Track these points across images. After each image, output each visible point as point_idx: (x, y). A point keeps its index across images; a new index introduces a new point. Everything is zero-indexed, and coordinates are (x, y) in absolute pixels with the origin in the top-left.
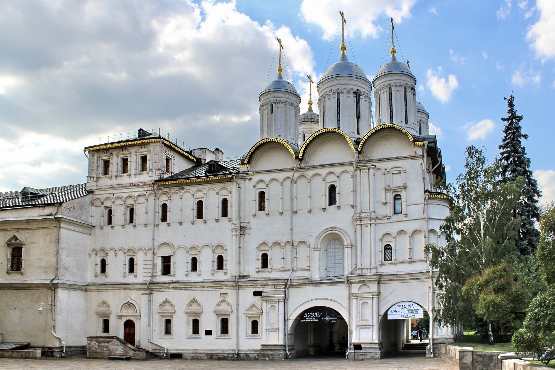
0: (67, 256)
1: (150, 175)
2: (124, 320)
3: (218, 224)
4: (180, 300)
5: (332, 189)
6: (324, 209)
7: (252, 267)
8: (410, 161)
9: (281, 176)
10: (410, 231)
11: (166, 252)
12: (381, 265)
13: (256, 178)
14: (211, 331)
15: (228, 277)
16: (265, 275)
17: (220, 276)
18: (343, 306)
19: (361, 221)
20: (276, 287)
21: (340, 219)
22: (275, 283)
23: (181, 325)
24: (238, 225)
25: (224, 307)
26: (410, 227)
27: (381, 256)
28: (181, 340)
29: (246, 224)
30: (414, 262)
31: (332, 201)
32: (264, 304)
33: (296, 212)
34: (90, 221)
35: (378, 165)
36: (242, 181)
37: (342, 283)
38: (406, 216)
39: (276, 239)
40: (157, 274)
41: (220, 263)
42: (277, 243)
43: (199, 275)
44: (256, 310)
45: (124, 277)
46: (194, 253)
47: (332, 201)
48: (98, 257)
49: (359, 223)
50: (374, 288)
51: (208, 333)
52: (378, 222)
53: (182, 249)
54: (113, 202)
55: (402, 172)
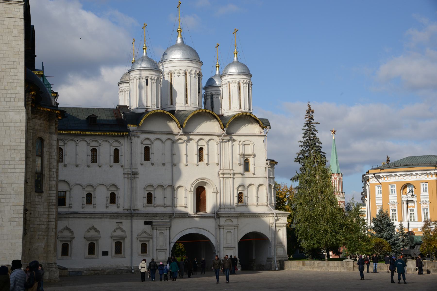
3: (112, 168)
4: (80, 228)
7: (140, 203)
8: (257, 137)
10: (257, 185)
14: (108, 252)
15: (120, 210)
16: (150, 209)
17: (113, 208)
18: (211, 234)
19: (223, 175)
20: (162, 218)
22: (162, 215)
24: (130, 170)
25: (119, 233)
28: (79, 260)
29: (136, 171)
30: (260, 205)
32: (155, 231)
36: (133, 138)
38: (254, 174)
39: (160, 182)
41: (113, 198)
42: (161, 186)
43: (95, 207)
44: (146, 235)
46: (90, 189)
47: (200, 158)
51: (105, 253)
53: (79, 187)
55: (251, 144)
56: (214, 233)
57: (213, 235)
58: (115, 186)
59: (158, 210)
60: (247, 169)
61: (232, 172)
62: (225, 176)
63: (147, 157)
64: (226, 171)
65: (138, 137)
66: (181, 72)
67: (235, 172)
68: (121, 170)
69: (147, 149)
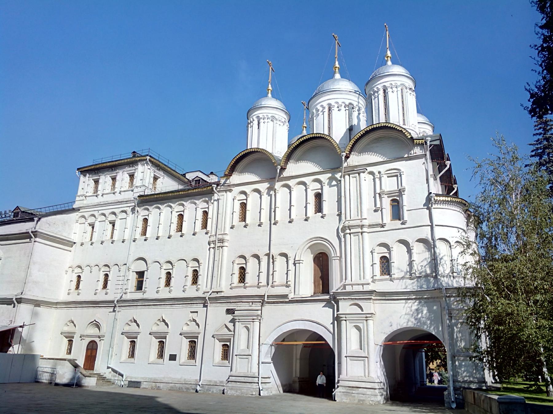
0: (39, 271)
1: (134, 191)
4: (148, 318)
11: (141, 266)
15: (200, 294)
20: (251, 303)
21: (326, 228)
23: (147, 347)
25: (193, 328)
26: (410, 236)
34: (72, 238)
35: (370, 169)
40: (128, 291)
48: (74, 274)
49: (348, 231)
51: (173, 358)
57: (330, 333)
58: (197, 260)
62: (352, 231)
64: (352, 223)
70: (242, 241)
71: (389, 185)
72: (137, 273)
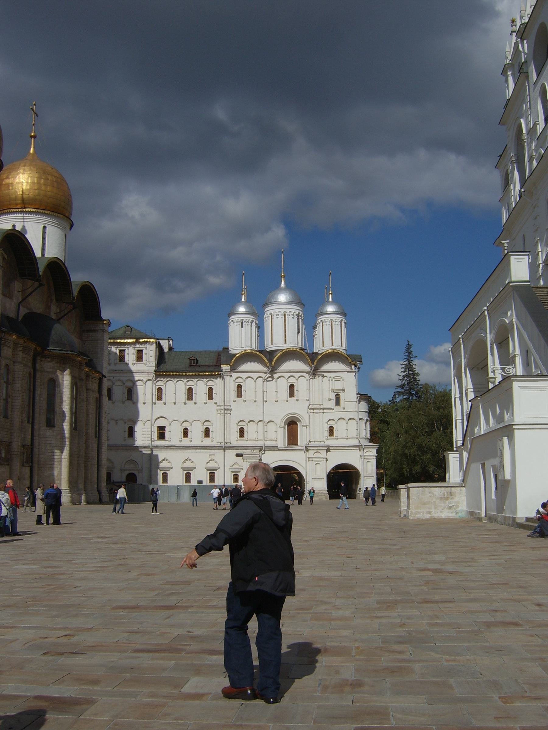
2: (127, 473)
5: (292, 386)
6: (287, 401)
9: (255, 376)
10: (347, 419)
12: (327, 439)
13: (235, 375)
15: (214, 444)
17: (207, 442)
25: (212, 465)
26: (347, 416)
27: (327, 433)
29: (228, 407)
31: (292, 394)
33: (266, 401)
35: (325, 374)
37: (302, 450)
41: (207, 433)
43: (191, 441)
45: (125, 440)
47: (292, 394)
50: (323, 453)
52: (325, 411)
54: (113, 383)
56: (304, 465)
59: (250, 443)
60: (338, 403)
61: (322, 407)
62: (315, 411)
63: (239, 395)
64: (315, 406)
65: (231, 376)
66: (279, 313)
67: (325, 406)
68: (215, 407)
69: (239, 387)
70: (241, 411)
71: (338, 386)
72: (158, 427)
